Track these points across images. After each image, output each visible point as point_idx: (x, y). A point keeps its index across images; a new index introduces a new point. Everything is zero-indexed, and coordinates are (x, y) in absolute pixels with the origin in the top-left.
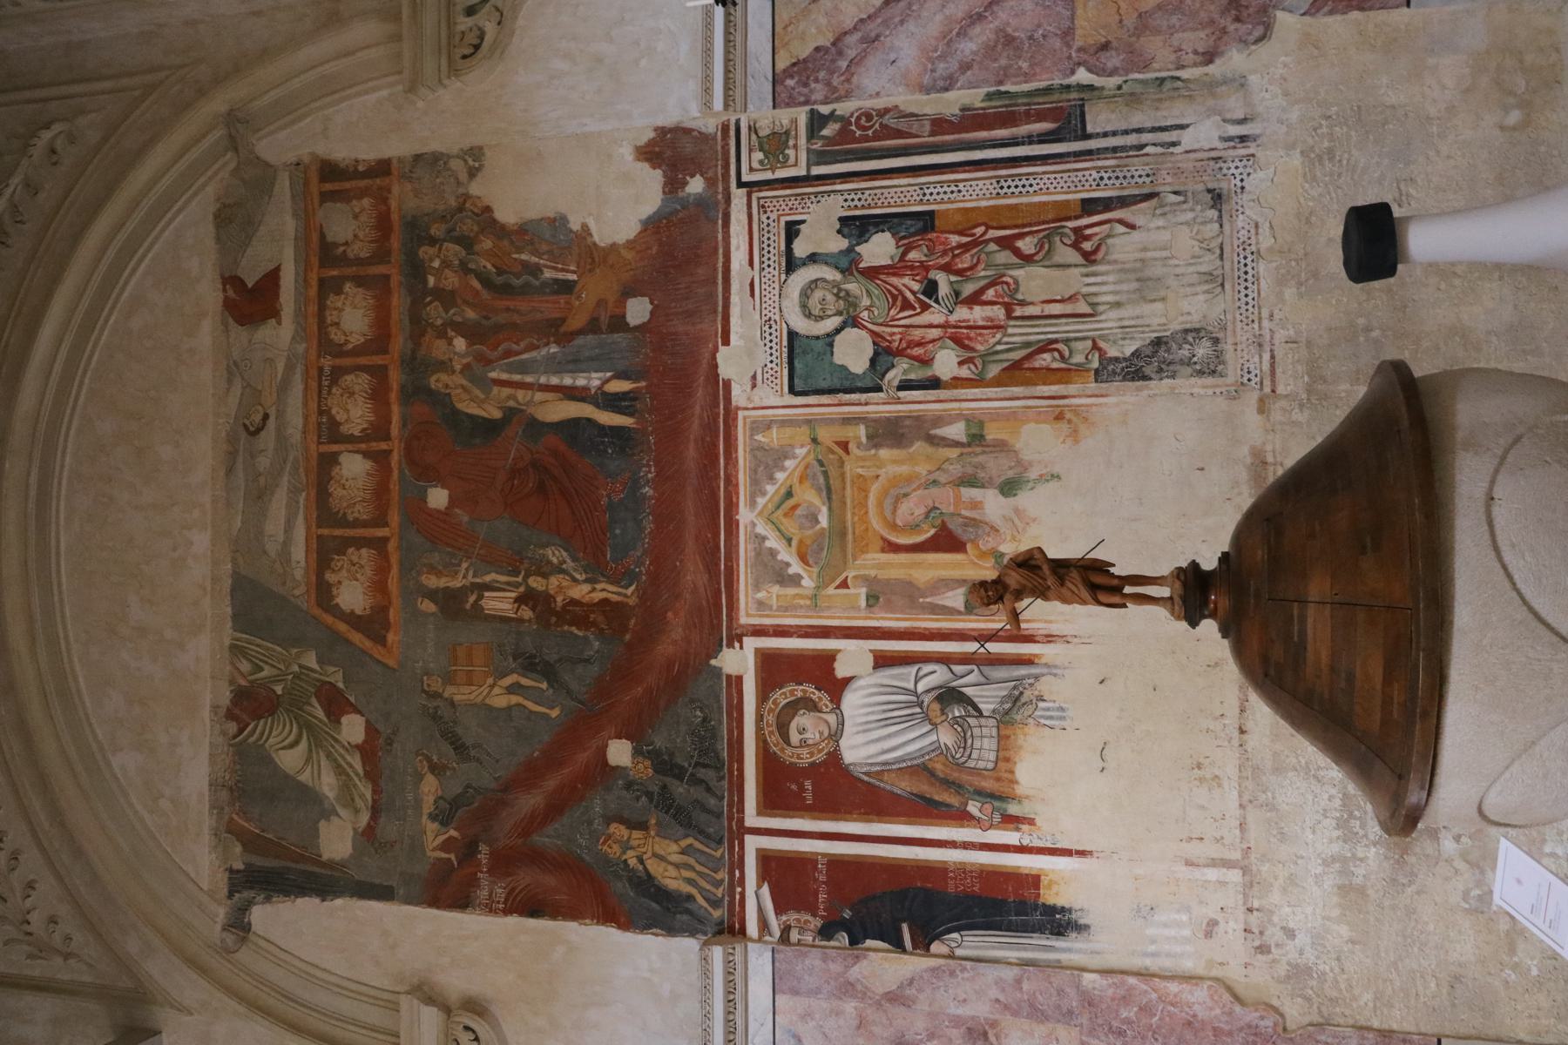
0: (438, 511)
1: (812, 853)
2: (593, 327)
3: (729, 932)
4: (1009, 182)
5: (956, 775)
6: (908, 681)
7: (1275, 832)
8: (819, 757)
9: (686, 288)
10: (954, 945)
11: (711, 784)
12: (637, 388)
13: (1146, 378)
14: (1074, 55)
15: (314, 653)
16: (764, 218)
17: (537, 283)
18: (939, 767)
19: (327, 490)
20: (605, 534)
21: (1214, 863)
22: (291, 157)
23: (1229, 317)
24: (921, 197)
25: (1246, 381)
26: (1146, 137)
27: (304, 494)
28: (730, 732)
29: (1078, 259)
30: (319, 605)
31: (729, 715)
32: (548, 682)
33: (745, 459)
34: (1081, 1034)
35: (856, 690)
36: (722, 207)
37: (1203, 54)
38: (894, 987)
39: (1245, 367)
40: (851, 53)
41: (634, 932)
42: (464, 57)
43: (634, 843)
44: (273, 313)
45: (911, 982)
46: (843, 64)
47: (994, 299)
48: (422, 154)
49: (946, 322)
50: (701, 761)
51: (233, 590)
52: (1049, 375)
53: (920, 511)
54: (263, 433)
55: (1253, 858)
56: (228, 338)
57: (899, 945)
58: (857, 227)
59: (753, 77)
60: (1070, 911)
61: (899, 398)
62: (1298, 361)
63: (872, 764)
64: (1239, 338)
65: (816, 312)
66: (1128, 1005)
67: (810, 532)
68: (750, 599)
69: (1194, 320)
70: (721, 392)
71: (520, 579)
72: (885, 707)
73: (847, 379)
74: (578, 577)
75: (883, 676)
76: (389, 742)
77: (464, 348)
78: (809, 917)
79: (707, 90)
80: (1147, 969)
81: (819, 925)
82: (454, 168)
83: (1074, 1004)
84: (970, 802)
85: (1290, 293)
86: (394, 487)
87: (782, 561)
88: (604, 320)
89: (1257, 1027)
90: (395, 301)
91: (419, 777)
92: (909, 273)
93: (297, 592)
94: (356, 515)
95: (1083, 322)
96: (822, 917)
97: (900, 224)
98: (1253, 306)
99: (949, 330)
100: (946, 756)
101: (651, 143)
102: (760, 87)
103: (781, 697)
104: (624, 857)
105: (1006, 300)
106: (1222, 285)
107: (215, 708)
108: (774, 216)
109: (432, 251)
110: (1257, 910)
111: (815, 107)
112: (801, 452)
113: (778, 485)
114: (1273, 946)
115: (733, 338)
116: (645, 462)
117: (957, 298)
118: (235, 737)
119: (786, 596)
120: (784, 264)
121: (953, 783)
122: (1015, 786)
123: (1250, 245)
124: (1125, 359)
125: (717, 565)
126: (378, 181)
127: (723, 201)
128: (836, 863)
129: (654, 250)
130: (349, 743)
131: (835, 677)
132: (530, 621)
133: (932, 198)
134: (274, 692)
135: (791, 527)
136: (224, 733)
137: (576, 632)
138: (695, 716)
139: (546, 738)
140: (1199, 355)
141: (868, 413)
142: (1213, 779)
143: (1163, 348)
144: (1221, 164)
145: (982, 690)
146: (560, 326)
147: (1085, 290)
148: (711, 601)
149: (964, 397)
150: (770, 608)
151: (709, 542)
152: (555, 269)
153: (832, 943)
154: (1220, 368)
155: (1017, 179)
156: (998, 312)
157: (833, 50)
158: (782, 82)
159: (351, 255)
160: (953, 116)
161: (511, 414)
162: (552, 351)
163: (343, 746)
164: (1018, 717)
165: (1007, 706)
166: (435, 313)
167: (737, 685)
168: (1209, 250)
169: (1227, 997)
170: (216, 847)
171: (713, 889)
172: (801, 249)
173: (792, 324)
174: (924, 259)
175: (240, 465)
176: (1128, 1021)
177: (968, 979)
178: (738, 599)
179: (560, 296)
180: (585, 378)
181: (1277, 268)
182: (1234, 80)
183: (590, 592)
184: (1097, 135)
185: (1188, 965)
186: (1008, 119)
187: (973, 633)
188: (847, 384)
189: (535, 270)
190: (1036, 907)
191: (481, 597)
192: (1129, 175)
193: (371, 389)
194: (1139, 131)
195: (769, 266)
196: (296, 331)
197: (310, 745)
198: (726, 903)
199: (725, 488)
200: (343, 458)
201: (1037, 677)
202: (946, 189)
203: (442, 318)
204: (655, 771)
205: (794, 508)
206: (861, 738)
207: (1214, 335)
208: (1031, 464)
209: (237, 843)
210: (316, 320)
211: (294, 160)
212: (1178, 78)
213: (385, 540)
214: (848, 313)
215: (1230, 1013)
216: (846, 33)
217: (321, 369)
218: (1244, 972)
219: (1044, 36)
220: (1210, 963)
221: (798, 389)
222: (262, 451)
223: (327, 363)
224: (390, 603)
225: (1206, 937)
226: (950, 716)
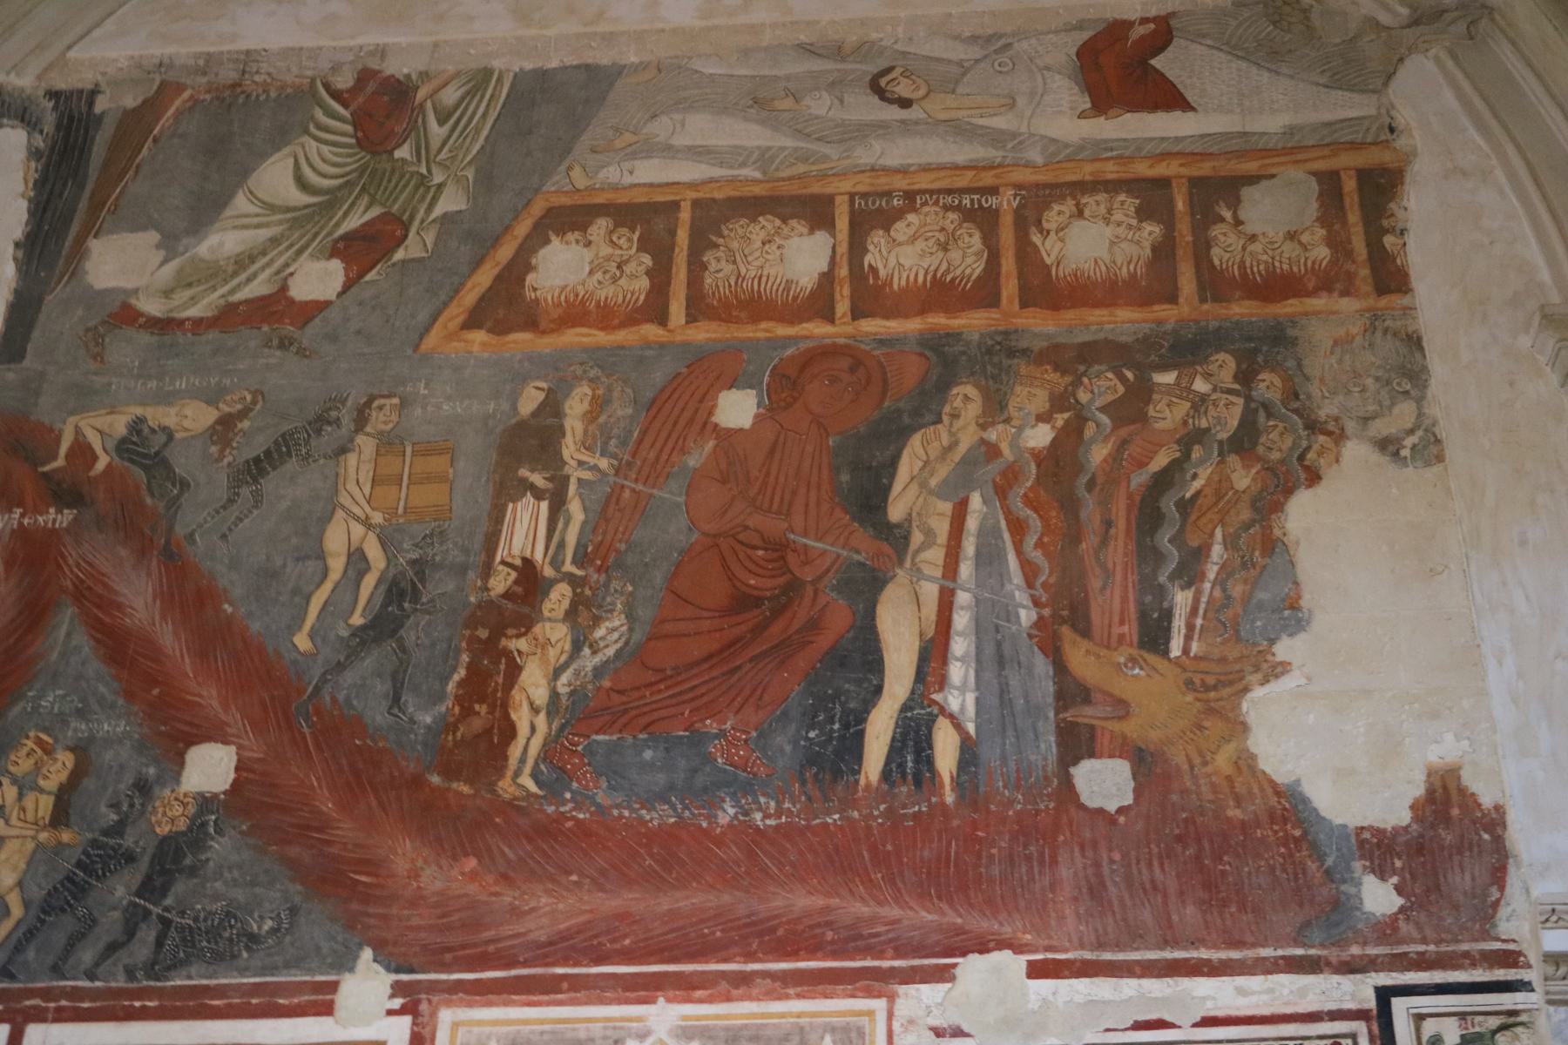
0: (711, 413)
2: (1071, 692)
9: (1153, 881)
12: (942, 786)
15: (464, 207)
17: (1162, 579)
19: (762, 214)
20: (645, 728)
22: (1405, 115)
27: (758, 175)
28: (221, 991)
30: (550, 211)
31: (256, 989)
32: (364, 628)
33: (782, 1015)
36: (1333, 954)
43: (29, 802)
44: (1102, 101)
48: (1421, 349)
50: (173, 933)
54: (876, 100)
56: (1056, 32)
68: (487, 1029)
70: (926, 962)
71: (569, 567)
74: (564, 678)
76: (285, 344)
77: (1032, 444)
82: (1396, 410)
90: (1124, 314)
91: (212, 398)
93: (577, 173)
94: (713, 266)
101: (1469, 800)
107: (382, 52)
109: (1227, 376)
115: (1045, 986)
116: (787, 805)
118: (327, 86)
125: (565, 961)
126: (1365, 272)
127: (1345, 956)
129: (1233, 813)
130: (292, 274)
134: (398, 146)
136: (336, 68)
137: (456, 677)
138: (262, 918)
139: (255, 626)
146: (1074, 627)
148: (491, 948)
151: (613, 941)
152: (1194, 611)
159: (1216, 231)
161: (896, 538)
162: (1023, 613)
163: (287, 265)
166: (1102, 388)
170: (139, 66)
175: (817, 65)
178: (490, 1004)
179: (1135, 625)
183: (531, 704)
189: (1189, 573)
191: (539, 495)
193: (953, 280)
196: (1067, 146)
197: (295, 209)
199: (723, 974)
200: (822, 239)
203: (1092, 401)
204: (164, 840)
209: (139, 101)
210: (1088, 178)
211: (1400, 122)
213: (662, 319)
217: (993, 191)
222: (842, 101)
224: (543, 332)
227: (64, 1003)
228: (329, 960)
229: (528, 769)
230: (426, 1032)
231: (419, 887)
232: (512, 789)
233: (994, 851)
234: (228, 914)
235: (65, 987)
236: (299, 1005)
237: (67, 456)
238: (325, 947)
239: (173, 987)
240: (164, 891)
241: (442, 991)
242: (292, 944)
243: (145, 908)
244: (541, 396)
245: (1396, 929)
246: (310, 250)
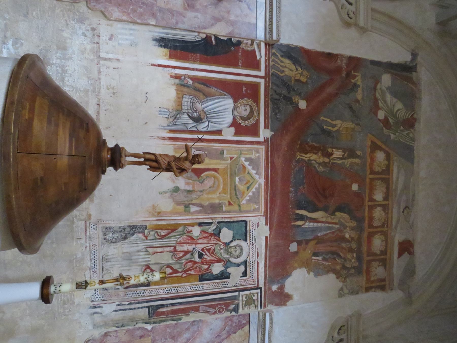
0: (355, 183)
2: (307, 242)
3: (270, 44)
4: (174, 291)
5: (196, 93)
6: (211, 125)
8: (240, 101)
10: (198, 36)
13: (130, 226)
14: (152, 334)
15: (392, 139)
16: (254, 278)
18: (201, 96)
21: (110, 60)
23: (100, 247)
24: (203, 286)
25: (95, 225)
26: (128, 307)
28: (268, 110)
29: (151, 266)
31: (268, 115)
32: (324, 128)
33: (262, 199)
34: (156, 4)
35: (228, 123)
36: (267, 281)
37: (108, 336)
38: (218, 23)
39: (95, 230)
40: (225, 332)
41: (299, 46)
42: (344, 326)
43: (299, 75)
45: (212, 25)
46: (227, 328)
47: (180, 253)
49: (196, 245)
51: (413, 158)
52: (162, 227)
53: (206, 182)
54: (404, 207)
57: (216, 37)
58: (224, 276)
59: (256, 323)
60: (159, 46)
61: (212, 220)
62: (77, 232)
64: (97, 240)
65: (238, 248)
67: (242, 175)
68: (261, 154)
69: (113, 246)
72: (219, 117)
73: (229, 226)
74: (314, 162)
78: (245, 48)
79: (271, 319)
83: (158, 14)
85: (79, 255)
86: (367, 191)
87: (251, 166)
88: (304, 244)
89: (96, 3)
91: (363, 99)
92: (208, 261)
93: (396, 158)
94: (379, 182)
95: (150, 245)
96: (240, 48)
97: (210, 277)
98: (92, 251)
99: (195, 242)
100: (199, 100)
102: (254, 320)
103: (252, 121)
104: (302, 70)
105: (176, 253)
106: (103, 258)
108: (251, 278)
110: (95, 43)
111: (236, 314)
112: (244, 202)
113: (251, 191)
116: (293, 198)
117: (192, 253)
118: (414, 113)
119: (249, 155)
120: (248, 263)
122: (176, 89)
123: (93, 272)
124: (136, 233)
125: (271, 165)
128: (235, 65)
129: (288, 266)
132: (329, 148)
133: (200, 285)
135: (248, 177)
140: (111, 234)
141: (222, 215)
143: (123, 237)
144: (103, 299)
145: (186, 122)
147: (149, 256)
149: (190, 220)
150: (255, 151)
152: (318, 260)
154: (104, 230)
155: (171, 293)
156: (178, 248)
157: (230, 333)
158: (247, 322)
159: (378, 263)
160: (192, 313)
161: (333, 214)
162: (320, 234)
164: (175, 112)
165: (179, 116)
166: (354, 245)
168: (107, 270)
169: (106, 14)
172: (242, 268)
173: (246, 244)
174: (203, 266)
176: (140, 7)
180: (310, 225)
181: (84, 264)
182: (98, 327)
183: (310, 157)
184: (144, 307)
185: (119, 25)
186: (174, 312)
187: (189, 141)
188: (229, 224)
189: (324, 259)
190: (170, 48)
191: (343, 155)
192: (134, 295)
194: (130, 309)
195: (252, 262)
197: (393, 110)
199: (268, 190)
201: (168, 125)
202: (195, 289)
205: (246, 184)
206: (227, 107)
207: (106, 241)
208: (169, 198)
212: (117, 327)
213: (371, 173)
214: (228, 247)
215: (105, 8)
216: (226, 338)
217: (387, 227)
219: (162, 340)
220: (112, 25)
221: (245, 222)
223: (385, 229)
225: (113, 35)
226: (197, 113)
229: (300, 157)
232: (297, 155)
233: (284, 231)
237: (354, 74)
240: (284, 99)
244: (359, 155)
245: (270, 290)
246: (386, 113)
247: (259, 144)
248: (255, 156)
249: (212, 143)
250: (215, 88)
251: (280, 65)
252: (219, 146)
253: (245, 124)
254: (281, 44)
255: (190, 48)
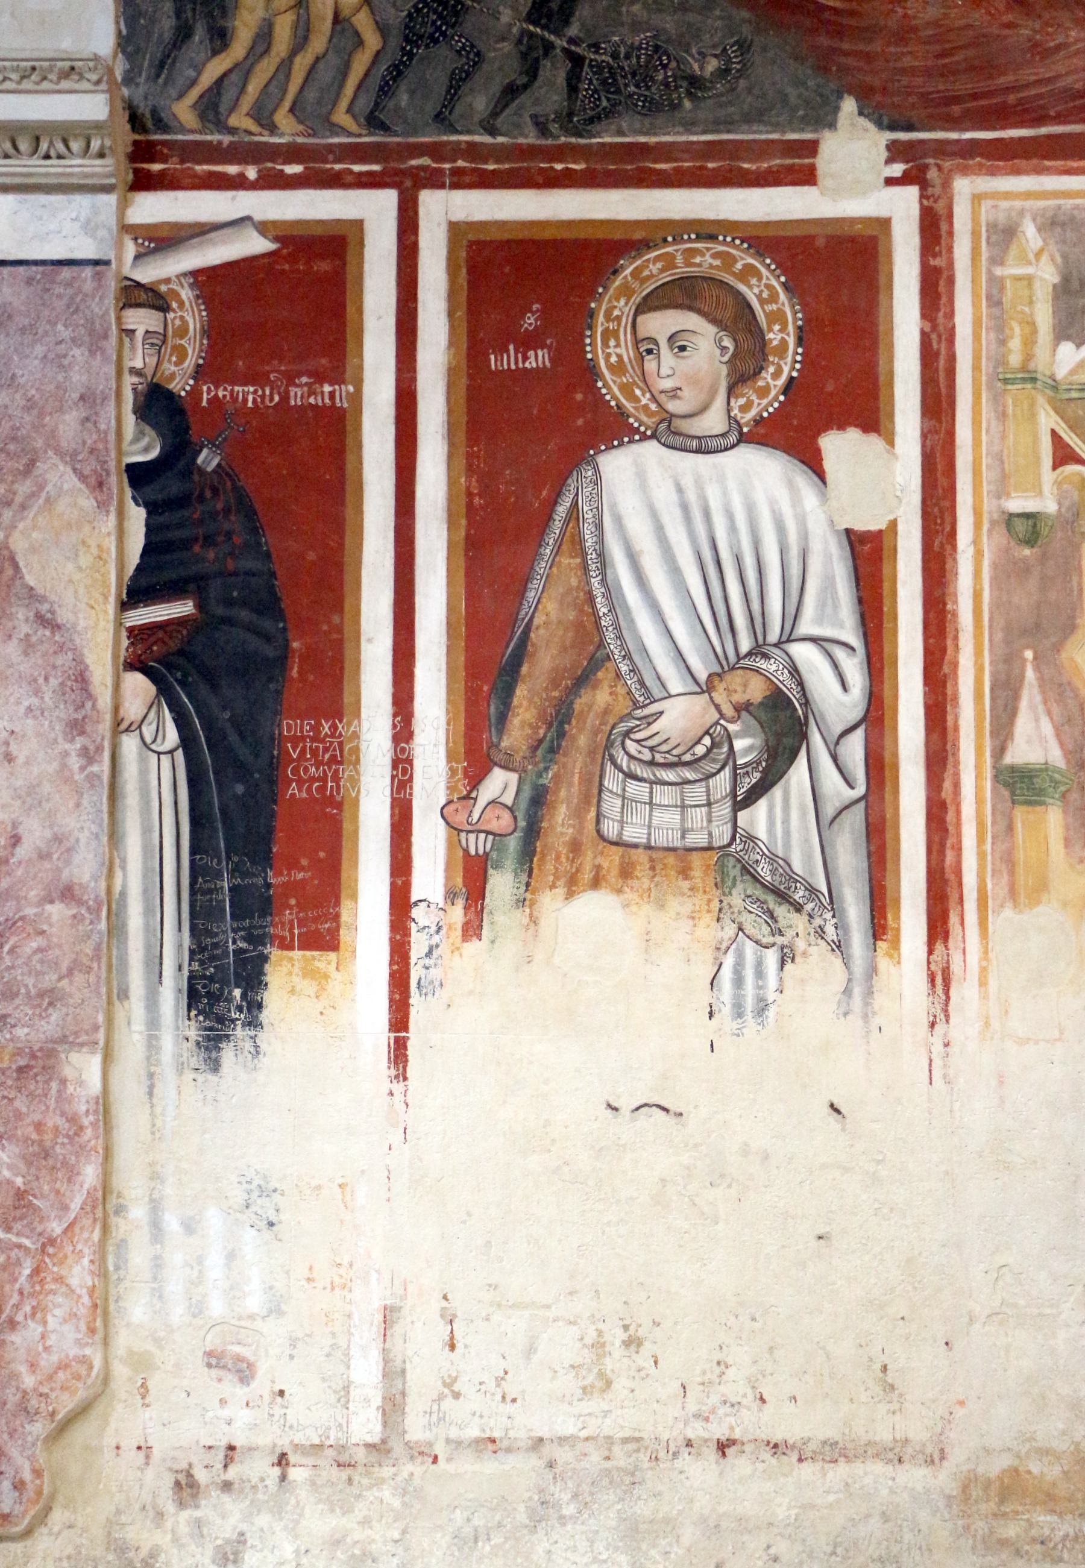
1: (360, 368)
3: (136, 143)
5: (583, 741)
6: (819, 620)
7: (478, 1521)
8: (611, 388)
10: (148, 731)
11: (524, 98)
31: (710, 150)
35: (791, 485)
38: (30, 580)
45: (46, 621)
55: (408, 1468)
60: (253, 1023)
63: (599, 526)
66: (29, 1164)
68: (1018, 204)
75: (828, 557)
78: (190, 363)
80: (120, 1210)
81: (174, 386)
83: (21, 1032)
84: (513, 777)
96: (195, 392)
100: (629, 716)
110: (283, 1478)
114: (198, 1513)
119: (1031, 303)
121: (561, 734)
131: (826, 427)
142: (601, 1375)
148: (1012, 98)
150: (997, 260)
153: (130, 420)
164: (736, 899)
165: (764, 871)
167: (790, 169)
169: (66, 1404)
171: (247, 102)
177: (64, 766)
178: (1017, 172)
187: (947, 785)
190: (256, 939)
198: (214, 138)
201: (839, 947)
218: (129, 1444)
220: (142, 1363)
225: (209, 1354)
226: (731, 727)
227: (460, 163)
228: (801, 113)
230: (940, 207)
231: (905, 16)
234: (657, 48)
235: (459, 143)
236: (769, 171)
238: (792, 92)
239: (603, 145)
240: (566, 17)
241: (954, 154)
242: (749, 90)
243: (543, 39)
247: (944, 227)
248: (1038, 255)
249: (955, 614)
250: (531, 595)
251: (294, 53)
252: (971, 551)
253: (791, 341)
254: (126, 43)
255: (240, 789)
